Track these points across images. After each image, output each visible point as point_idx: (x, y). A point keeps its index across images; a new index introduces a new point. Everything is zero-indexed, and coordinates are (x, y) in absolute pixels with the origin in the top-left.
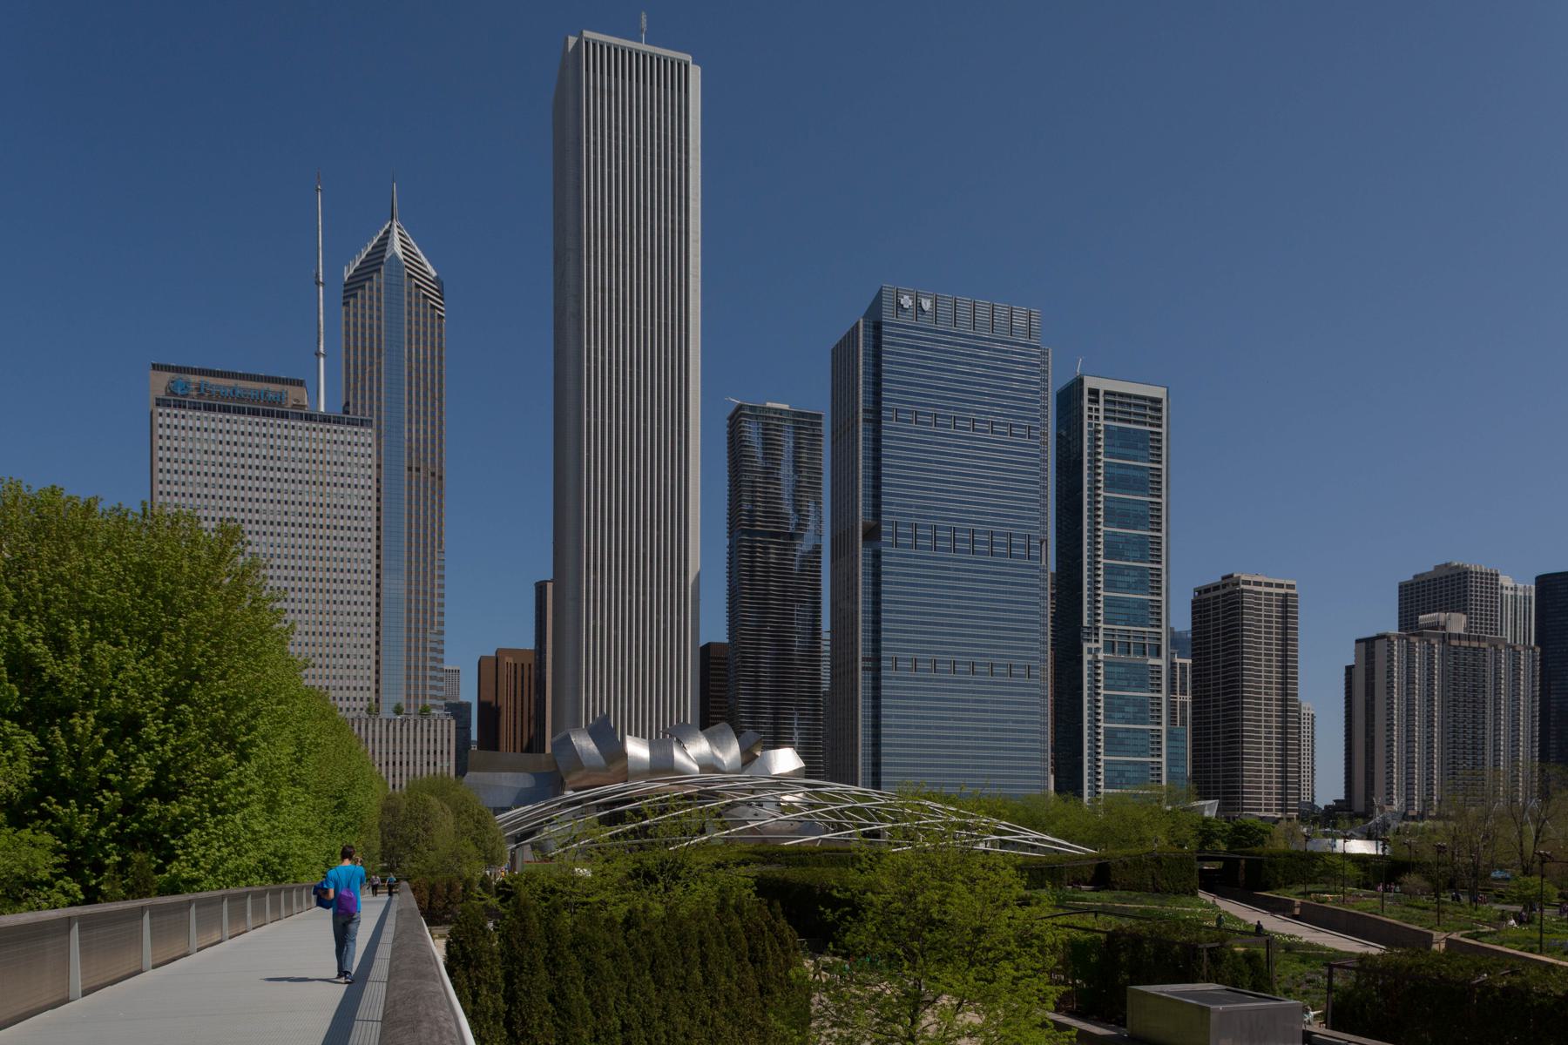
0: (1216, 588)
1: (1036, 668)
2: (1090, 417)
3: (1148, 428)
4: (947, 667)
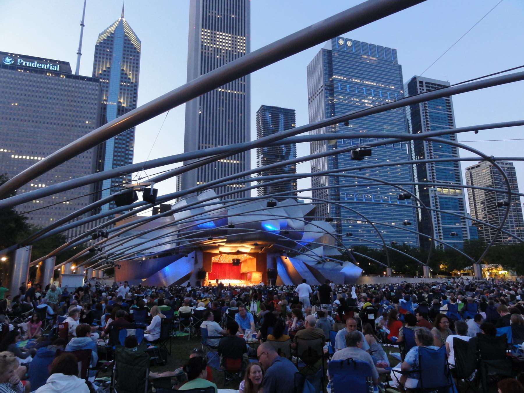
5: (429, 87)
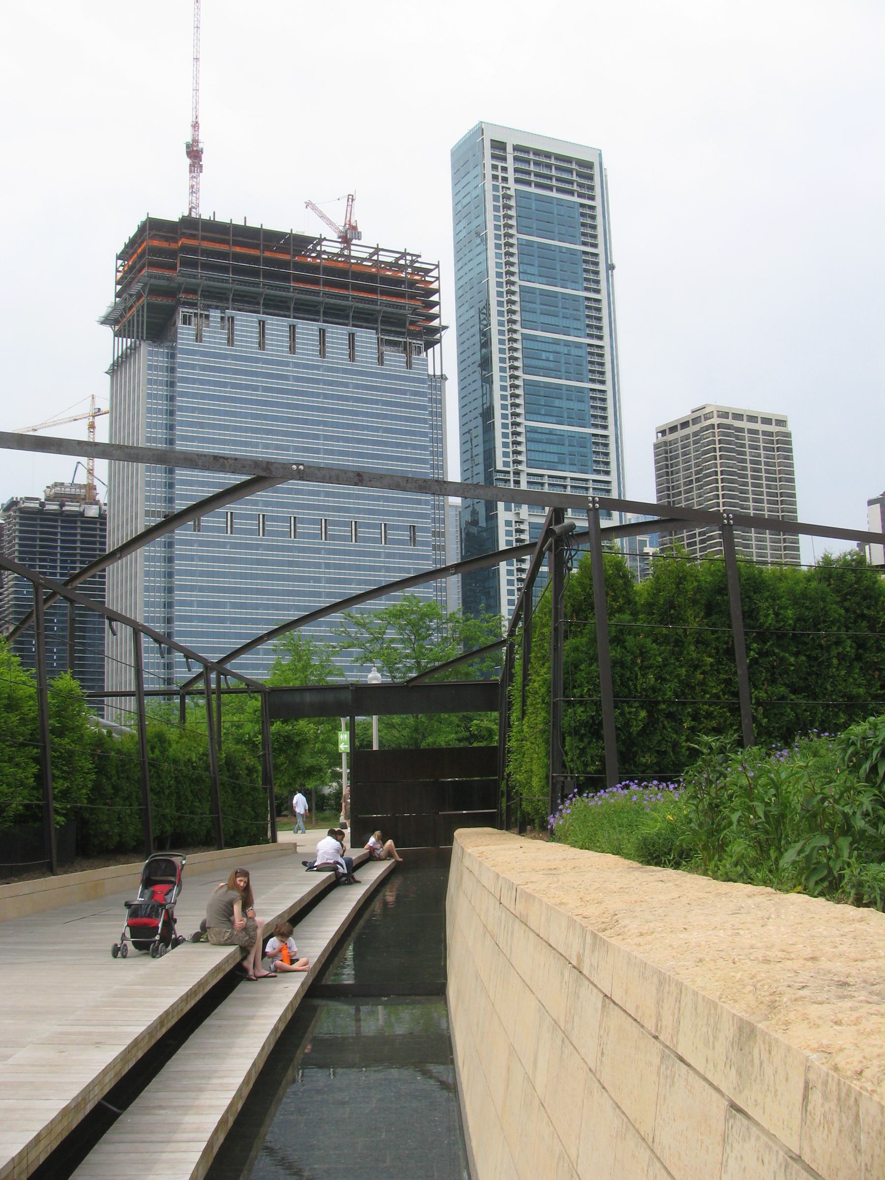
0: (685, 425)
1: (425, 530)
2: (495, 177)
3: (575, 199)
4: (283, 527)
5: (527, 162)
